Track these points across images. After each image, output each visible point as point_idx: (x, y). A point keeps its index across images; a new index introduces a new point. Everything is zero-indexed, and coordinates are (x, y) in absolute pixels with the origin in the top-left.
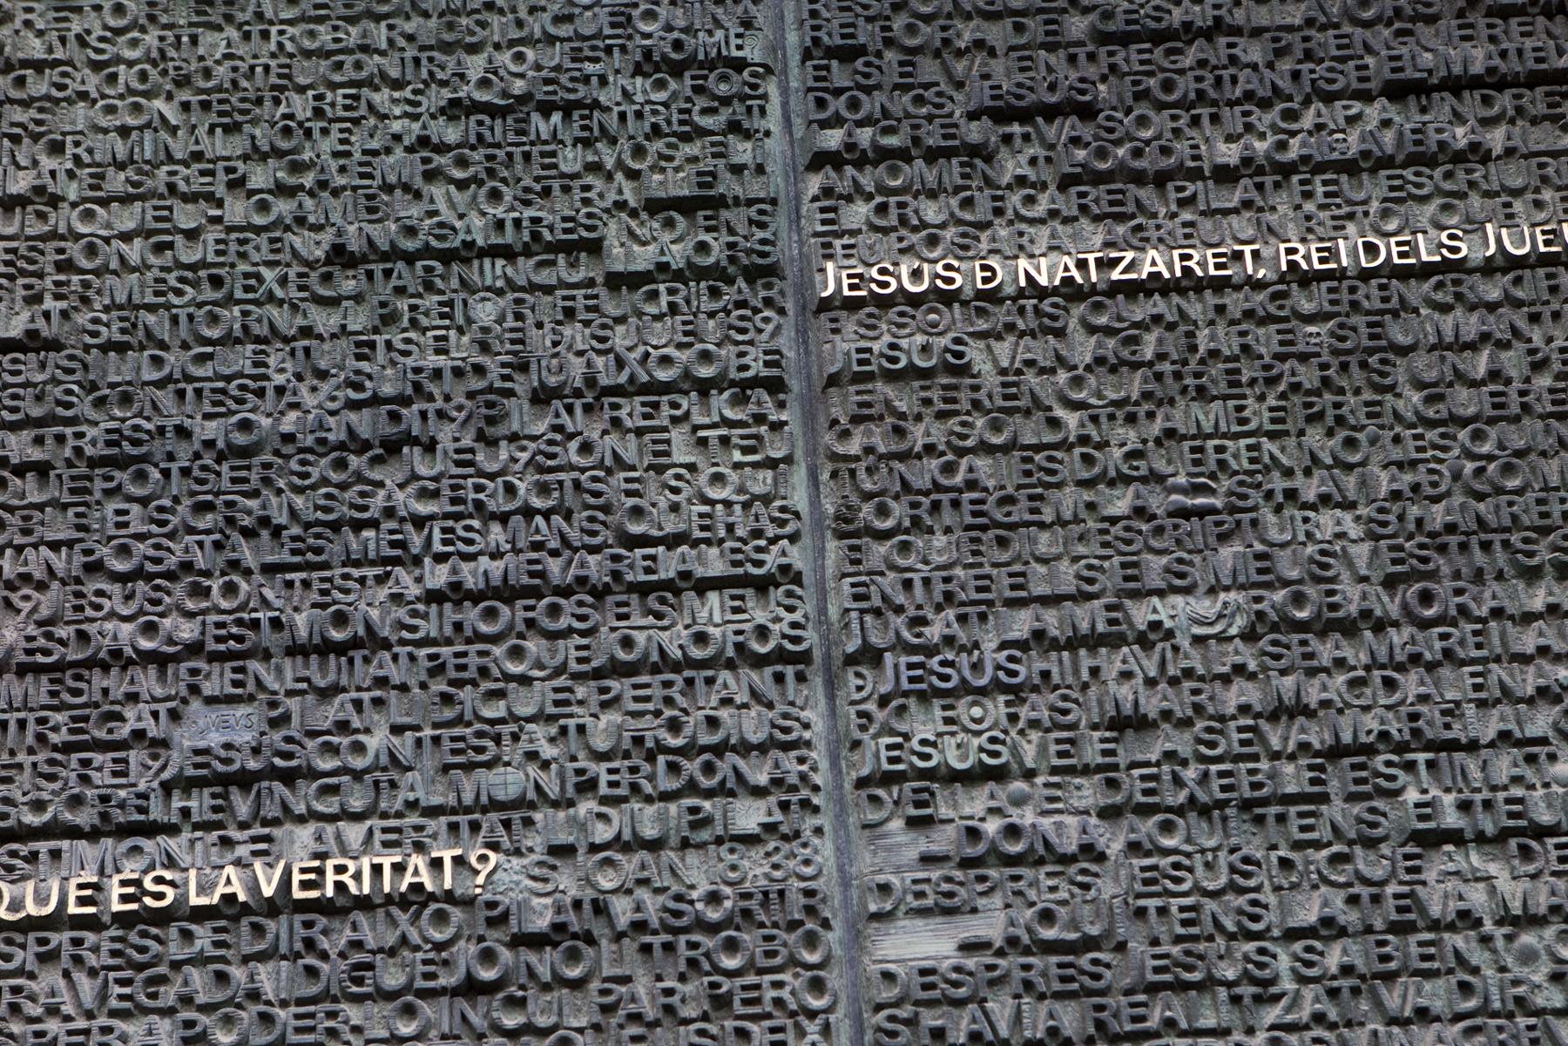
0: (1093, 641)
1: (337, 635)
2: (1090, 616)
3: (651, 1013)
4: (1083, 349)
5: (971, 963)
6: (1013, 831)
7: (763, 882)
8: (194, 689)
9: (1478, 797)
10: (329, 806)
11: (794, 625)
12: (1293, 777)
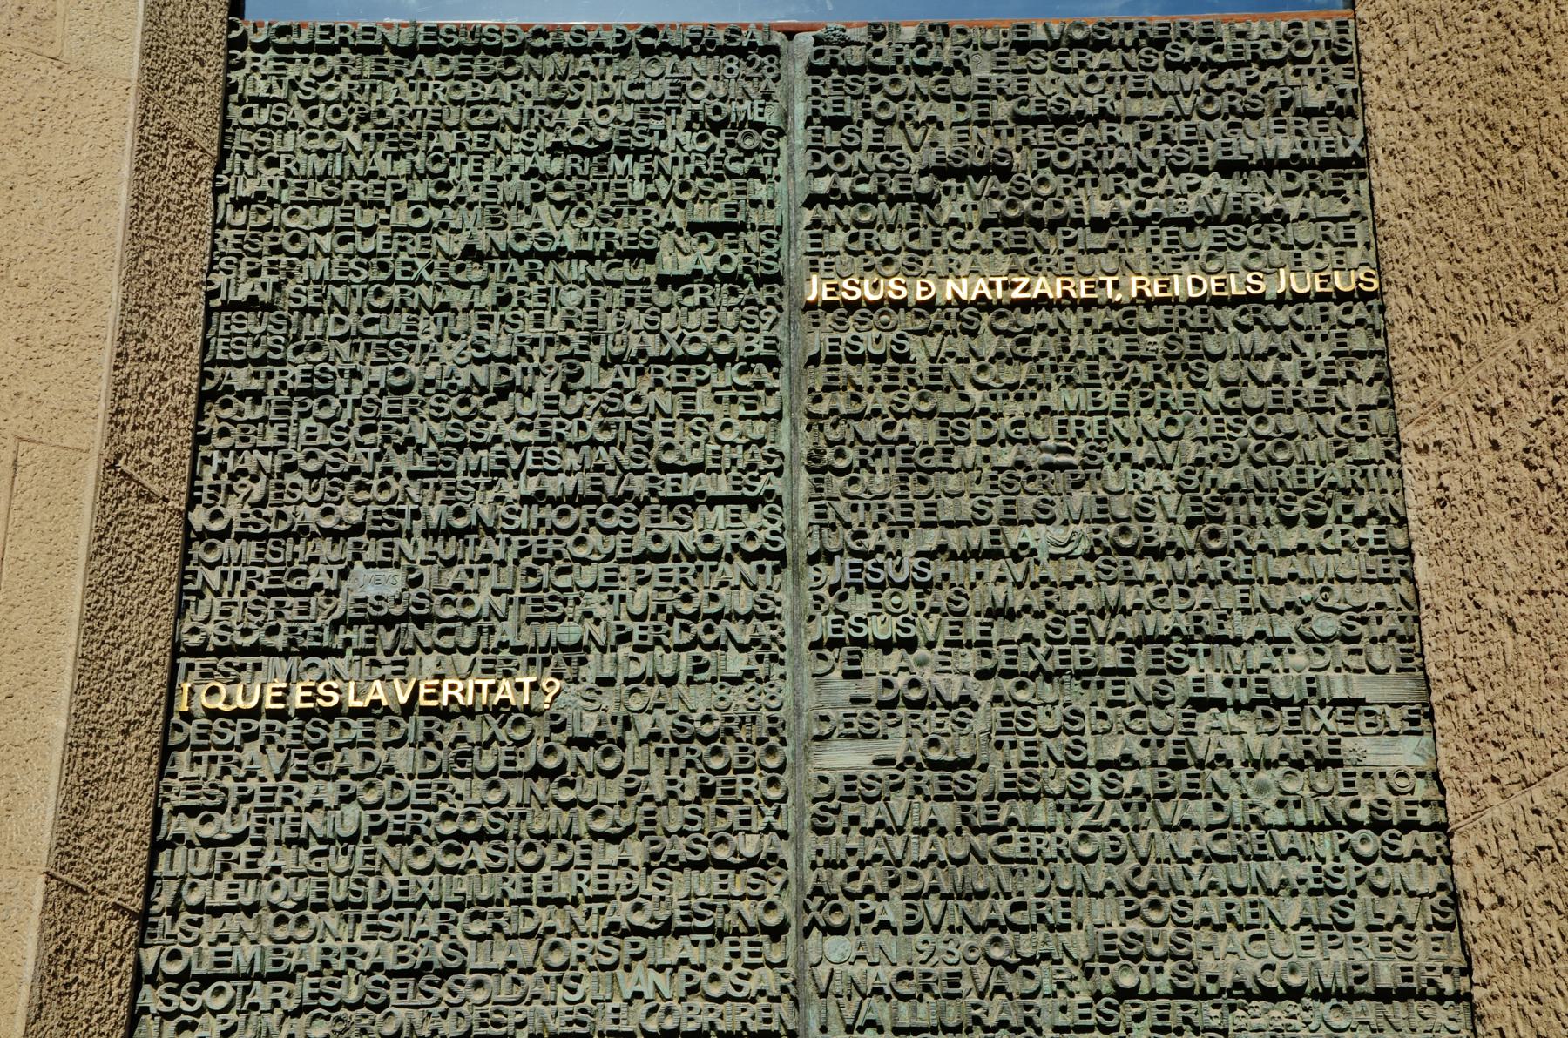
0: (977, 554)
1: (460, 523)
2: (978, 537)
3: (660, 797)
4: (989, 345)
5: (881, 772)
8: (357, 556)
9: (1237, 677)
10: (447, 642)
11: (774, 533)
12: (1111, 656)
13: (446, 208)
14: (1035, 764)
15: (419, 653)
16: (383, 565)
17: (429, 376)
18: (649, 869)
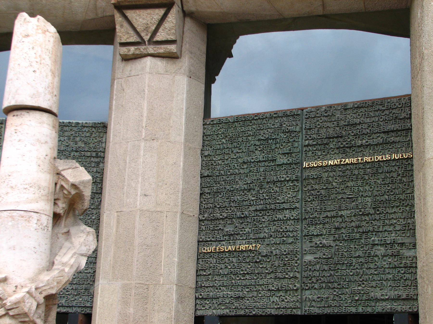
0: (334, 217)
1: (243, 216)
3: (277, 266)
7: (292, 249)
8: (227, 223)
11: (297, 215)
17: (237, 188)
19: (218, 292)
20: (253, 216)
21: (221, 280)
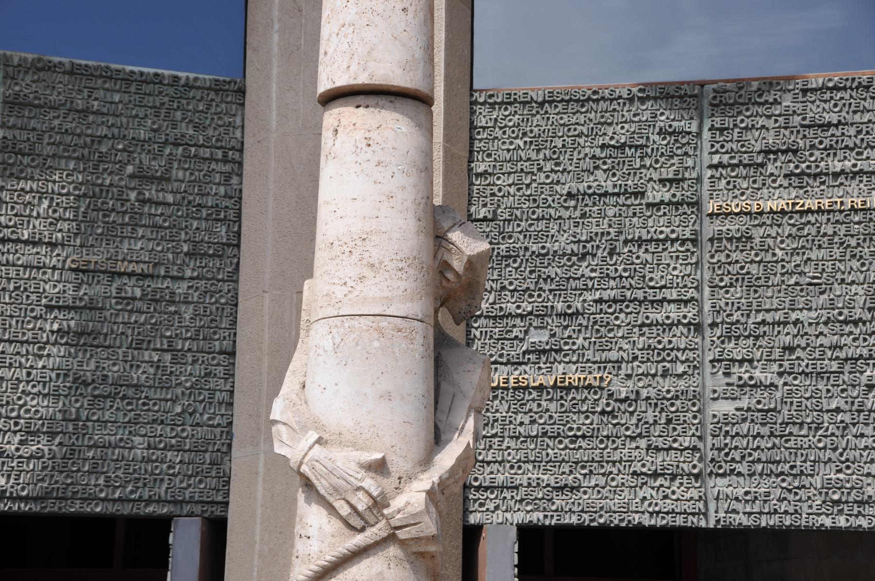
1: (569, 311)
2: (779, 316)
4: (787, 230)
5: (738, 413)
6: (751, 378)
7: (682, 387)
8: (530, 324)
12: (834, 365)
13: (559, 173)
14: (801, 411)
15: (556, 364)
16: (541, 328)
18: (648, 450)
19: (516, 474)
20: (593, 314)
21: (521, 449)
